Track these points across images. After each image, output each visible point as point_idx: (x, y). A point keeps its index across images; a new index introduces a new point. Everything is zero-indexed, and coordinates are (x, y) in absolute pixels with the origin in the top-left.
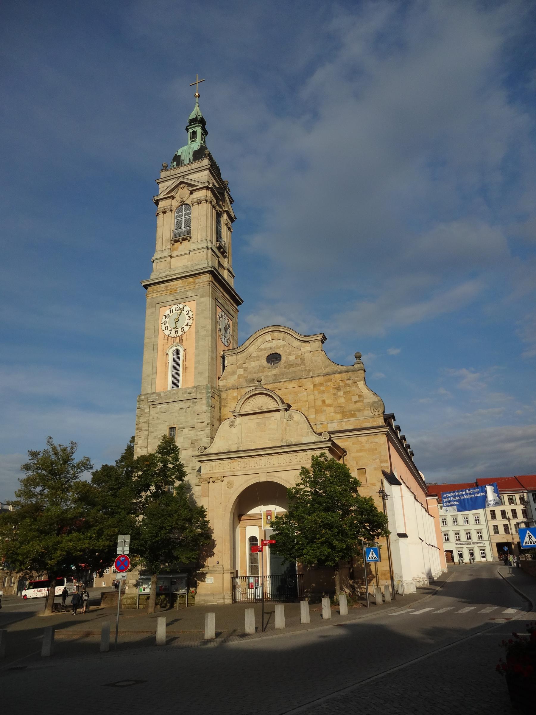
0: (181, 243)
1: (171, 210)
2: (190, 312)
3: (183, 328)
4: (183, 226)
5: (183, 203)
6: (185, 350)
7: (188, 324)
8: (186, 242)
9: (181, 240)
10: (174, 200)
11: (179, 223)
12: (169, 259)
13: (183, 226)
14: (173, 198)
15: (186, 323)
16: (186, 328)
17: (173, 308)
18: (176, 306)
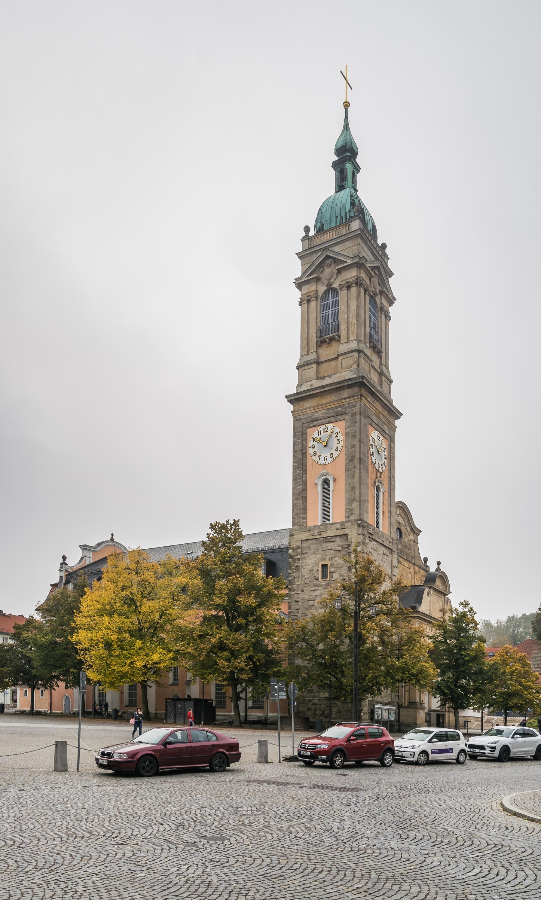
0: (329, 344)
1: (317, 298)
2: (339, 435)
3: (332, 454)
4: (330, 321)
5: (331, 290)
6: (335, 480)
7: (337, 450)
8: (334, 344)
9: (327, 340)
10: (319, 283)
11: (325, 319)
12: (314, 366)
13: (330, 321)
14: (318, 279)
15: (335, 448)
16: (336, 454)
17: (321, 428)
18: (324, 426)
